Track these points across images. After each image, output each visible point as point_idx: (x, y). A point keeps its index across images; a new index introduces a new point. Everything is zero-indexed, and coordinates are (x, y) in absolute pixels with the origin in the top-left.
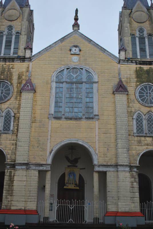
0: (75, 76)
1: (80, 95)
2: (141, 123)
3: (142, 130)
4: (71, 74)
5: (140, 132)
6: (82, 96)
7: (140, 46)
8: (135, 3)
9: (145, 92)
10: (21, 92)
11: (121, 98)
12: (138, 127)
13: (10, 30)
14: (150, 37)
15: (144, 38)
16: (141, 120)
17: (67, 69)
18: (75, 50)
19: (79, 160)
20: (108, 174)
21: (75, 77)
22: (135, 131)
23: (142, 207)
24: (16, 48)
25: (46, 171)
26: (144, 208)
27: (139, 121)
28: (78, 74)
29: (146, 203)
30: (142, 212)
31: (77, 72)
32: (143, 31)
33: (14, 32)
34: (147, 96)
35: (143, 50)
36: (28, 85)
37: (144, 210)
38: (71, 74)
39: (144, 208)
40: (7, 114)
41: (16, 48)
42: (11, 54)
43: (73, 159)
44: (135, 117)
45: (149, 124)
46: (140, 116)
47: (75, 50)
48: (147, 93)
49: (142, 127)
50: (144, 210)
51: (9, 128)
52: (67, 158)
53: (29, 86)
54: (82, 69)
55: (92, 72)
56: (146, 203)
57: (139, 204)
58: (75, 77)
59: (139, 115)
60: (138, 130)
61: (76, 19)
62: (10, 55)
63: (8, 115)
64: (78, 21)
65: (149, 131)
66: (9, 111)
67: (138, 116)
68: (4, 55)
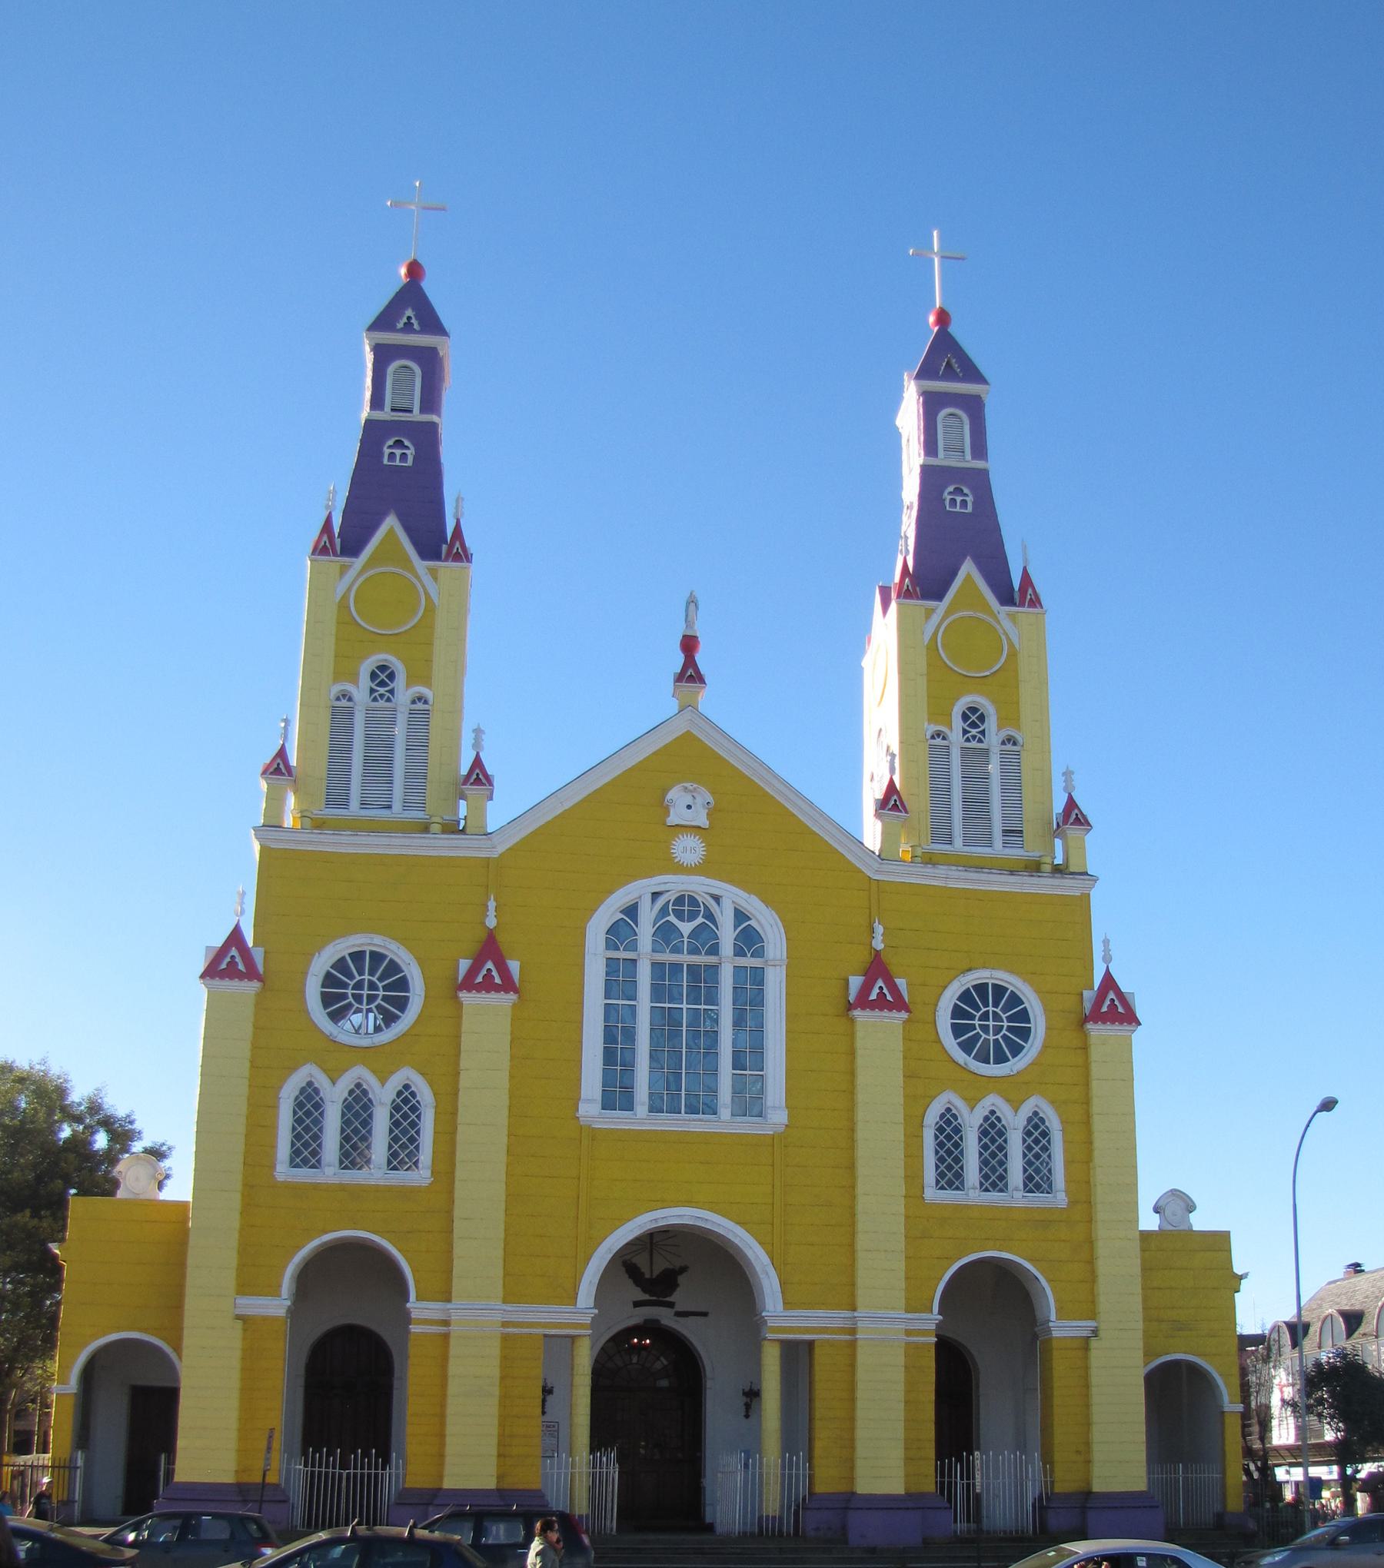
0: (686, 928)
1: (711, 1018)
2: (957, 1145)
3: (959, 1176)
4: (672, 918)
5: (950, 1184)
6: (716, 1021)
7: (964, 790)
8: (954, 574)
9: (978, 1009)
10: (456, 997)
11: (879, 1035)
12: (941, 1160)
13: (382, 684)
14: (1009, 747)
15: (986, 752)
16: (957, 1130)
17: (656, 895)
18: (689, 807)
20: (817, 1351)
21: (686, 935)
22: (930, 1174)
23: (942, 1475)
24: (417, 777)
25: (573, 1338)
26: (950, 1476)
27: (949, 1138)
28: (700, 920)
29: (960, 1459)
30: (942, 1493)
31: (692, 916)
32: (982, 718)
33: (404, 693)
34: (985, 1028)
35: (976, 805)
36: (489, 970)
37: (950, 1483)
38: (672, 918)
39: (950, 1476)
40: (399, 1094)
41: (417, 777)
42: (397, 806)
43: (656, 1273)
44: (932, 1117)
45: (985, 1147)
46: (955, 1117)
47: (689, 807)
48: (985, 1017)
49: (957, 1160)
50: (950, 1483)
53: (495, 973)
54: (717, 899)
55: (760, 917)
56: (960, 1459)
57: (933, 1462)
58: (686, 935)
59: (948, 1110)
60: (942, 1175)
61: (689, 645)
62: (389, 807)
63: (406, 1101)
64: (700, 658)
65: (986, 1177)
66: (407, 1087)
67: (942, 1116)
68: (364, 805)
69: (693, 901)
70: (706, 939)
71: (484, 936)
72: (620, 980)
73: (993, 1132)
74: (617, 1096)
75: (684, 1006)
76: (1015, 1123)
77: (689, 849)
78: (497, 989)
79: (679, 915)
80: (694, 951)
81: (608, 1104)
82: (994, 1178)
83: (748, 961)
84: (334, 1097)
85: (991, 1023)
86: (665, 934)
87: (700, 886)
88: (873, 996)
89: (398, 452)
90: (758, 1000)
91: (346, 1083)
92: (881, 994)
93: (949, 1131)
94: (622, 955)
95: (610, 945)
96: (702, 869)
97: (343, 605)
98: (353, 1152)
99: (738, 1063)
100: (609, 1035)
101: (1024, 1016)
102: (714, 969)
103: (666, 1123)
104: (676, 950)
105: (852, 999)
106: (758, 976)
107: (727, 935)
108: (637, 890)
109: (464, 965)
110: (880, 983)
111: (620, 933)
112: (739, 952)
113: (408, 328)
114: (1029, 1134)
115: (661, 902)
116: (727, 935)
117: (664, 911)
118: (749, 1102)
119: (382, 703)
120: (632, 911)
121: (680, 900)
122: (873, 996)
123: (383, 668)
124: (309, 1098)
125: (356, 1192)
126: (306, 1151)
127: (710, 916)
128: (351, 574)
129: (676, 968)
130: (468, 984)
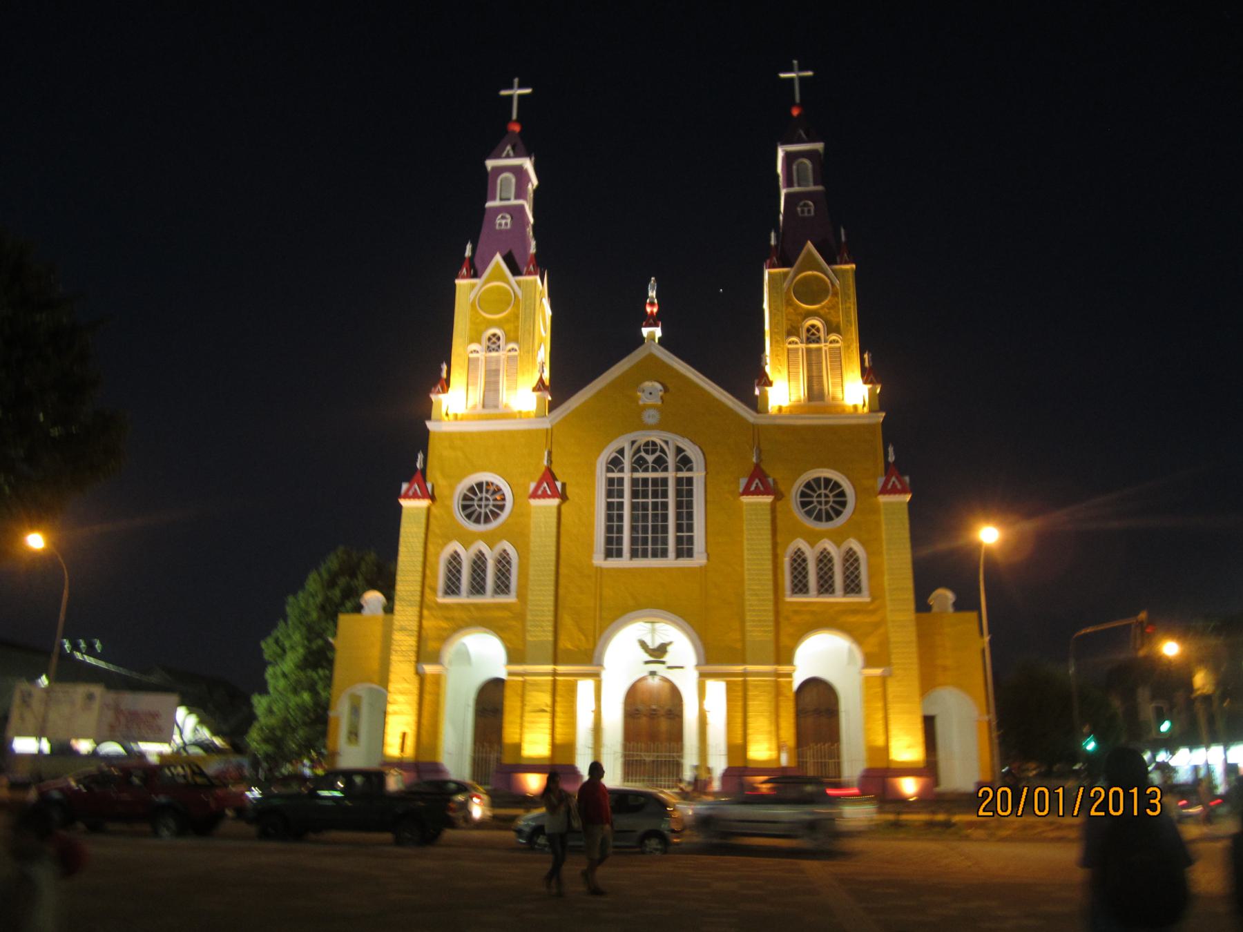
0: (650, 458)
4: (643, 454)
9: (814, 491)
16: (804, 560)
19: (669, 648)
28: (658, 453)
31: (654, 452)
34: (820, 503)
38: (643, 454)
43: (657, 644)
51: (507, 587)
52: (643, 644)
69: (654, 444)
70: (660, 463)
71: (543, 469)
72: (614, 488)
73: (824, 560)
74: (612, 549)
75: (650, 500)
76: (836, 554)
77: (651, 417)
78: (549, 497)
79: (647, 452)
80: (654, 470)
81: (608, 554)
82: (826, 586)
83: (684, 474)
84: (466, 558)
85: (823, 499)
86: (639, 464)
87: (656, 437)
88: (753, 488)
89: (503, 222)
90: (690, 493)
91: (473, 550)
92: (757, 487)
93: (799, 561)
94: (615, 475)
95: (609, 470)
96: (660, 426)
97: (473, 305)
98: (478, 587)
99: (679, 528)
100: (609, 518)
101: (842, 494)
102: (665, 481)
103: (640, 563)
104: (646, 470)
105: (741, 490)
106: (690, 481)
107: (671, 460)
108: (624, 442)
109: (533, 486)
110: (757, 481)
111: (615, 463)
112: (678, 469)
113: (508, 156)
114: (847, 560)
115: (636, 446)
116: (671, 460)
117: (638, 450)
118: (684, 549)
119: (494, 354)
120: (621, 452)
121: (647, 444)
122: (753, 488)
123: (494, 335)
124: (455, 559)
125: (477, 607)
126: (452, 587)
127: (663, 451)
128: (476, 289)
129: (645, 481)
130: (534, 495)
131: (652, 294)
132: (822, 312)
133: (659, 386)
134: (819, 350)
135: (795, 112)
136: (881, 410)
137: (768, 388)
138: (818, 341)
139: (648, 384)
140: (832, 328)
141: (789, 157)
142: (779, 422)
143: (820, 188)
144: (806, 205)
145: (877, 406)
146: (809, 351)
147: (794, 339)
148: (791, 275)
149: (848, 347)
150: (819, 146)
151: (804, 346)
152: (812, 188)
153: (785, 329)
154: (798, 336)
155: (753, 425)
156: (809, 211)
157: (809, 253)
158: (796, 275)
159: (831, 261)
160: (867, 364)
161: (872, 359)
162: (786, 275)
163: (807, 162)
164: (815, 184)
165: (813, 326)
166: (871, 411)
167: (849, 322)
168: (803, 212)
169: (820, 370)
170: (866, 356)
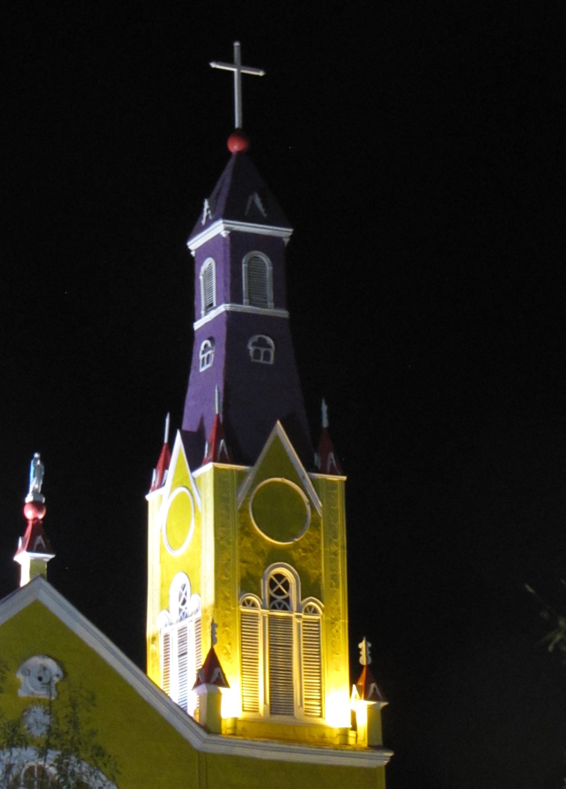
131: (34, 484)
132: (295, 555)
133: (51, 664)
134: (288, 621)
135: (235, 147)
136: (387, 745)
137: (222, 689)
138: (285, 605)
139: (37, 661)
140: (311, 588)
141: (238, 244)
142: (238, 751)
143: (283, 313)
144: (262, 343)
145: (380, 742)
146: (272, 620)
147: (254, 598)
148: (249, 479)
149: (332, 623)
150: (284, 233)
151: (267, 612)
152: (270, 310)
153: (237, 580)
154: (258, 593)
155: (199, 753)
156: (267, 356)
157: (277, 439)
158: (259, 478)
159: (310, 467)
160: (363, 660)
161: (373, 652)
162: (241, 475)
163: (265, 260)
164: (277, 305)
165: (279, 577)
166: (371, 746)
167: (334, 577)
168: (257, 352)
169: (289, 658)
170: (362, 645)
